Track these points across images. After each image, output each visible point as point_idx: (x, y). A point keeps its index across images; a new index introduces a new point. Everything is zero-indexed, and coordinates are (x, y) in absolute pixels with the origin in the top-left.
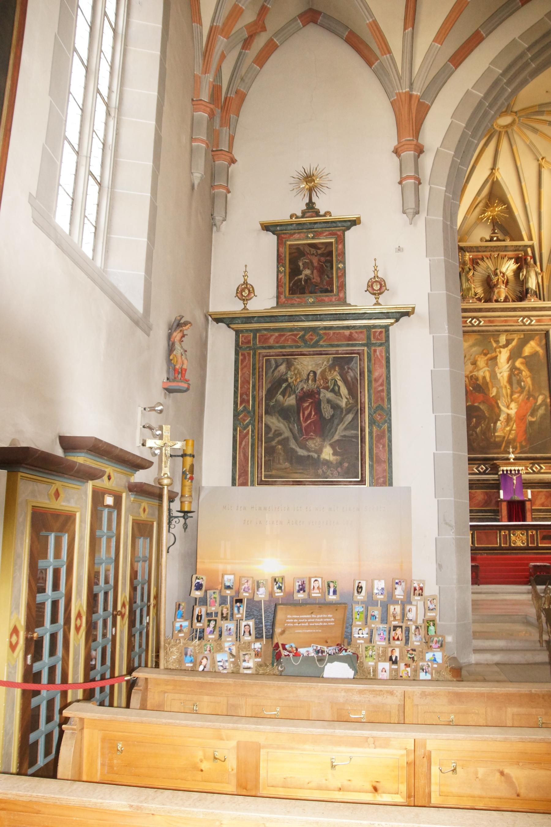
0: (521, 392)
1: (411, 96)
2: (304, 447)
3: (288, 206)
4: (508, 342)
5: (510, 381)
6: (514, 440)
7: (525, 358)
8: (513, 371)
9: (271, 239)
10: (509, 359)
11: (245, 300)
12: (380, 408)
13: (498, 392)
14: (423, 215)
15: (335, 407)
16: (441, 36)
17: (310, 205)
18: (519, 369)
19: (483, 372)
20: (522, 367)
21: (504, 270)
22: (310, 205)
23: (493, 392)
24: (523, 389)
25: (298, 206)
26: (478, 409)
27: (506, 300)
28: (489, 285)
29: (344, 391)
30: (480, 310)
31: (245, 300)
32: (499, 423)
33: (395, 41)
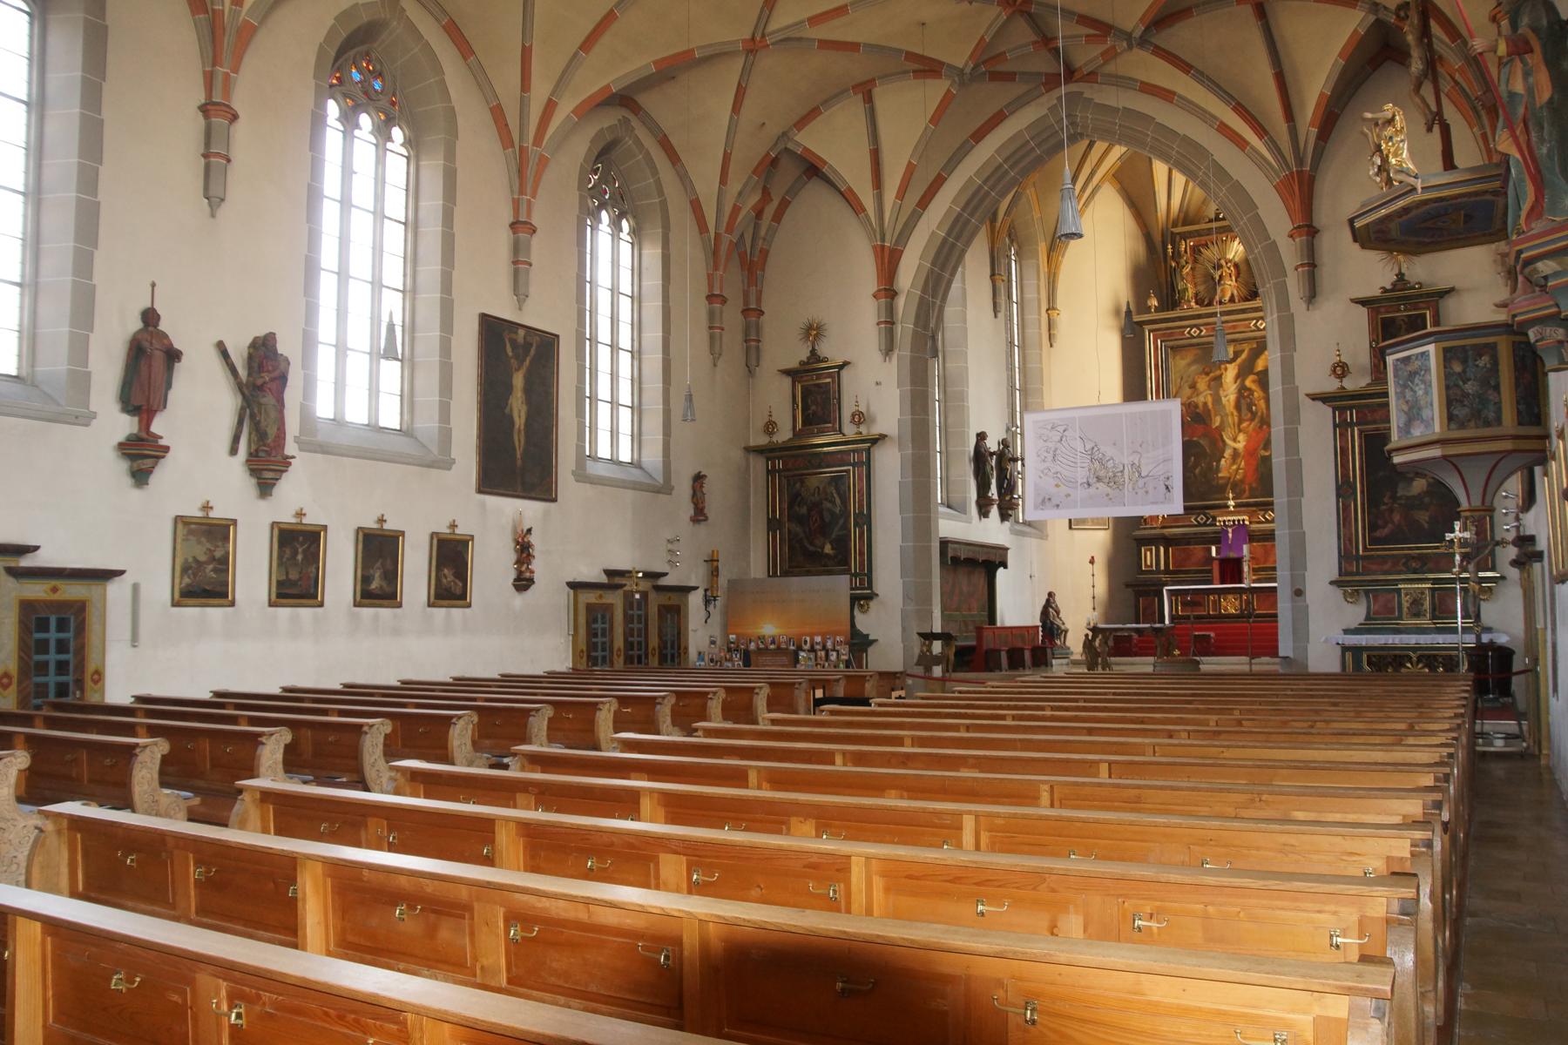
0: (1252, 420)
1: (883, 247)
2: (812, 544)
3: (797, 354)
4: (1237, 354)
5: (1238, 406)
6: (1242, 481)
7: (1257, 374)
8: (1243, 392)
9: (788, 381)
10: (1237, 377)
11: (771, 434)
12: (861, 512)
13: (1222, 422)
14: (896, 352)
15: (832, 513)
16: (901, 194)
17: (813, 352)
18: (1249, 389)
19: (1204, 397)
20: (1253, 387)
21: (1230, 256)
22: (813, 352)
23: (1217, 422)
24: (1254, 414)
25: (804, 354)
26: (1197, 444)
27: (1232, 300)
28: (1213, 283)
29: (838, 501)
30: (1199, 317)
31: (771, 434)
32: (1223, 462)
33: (868, 201)
